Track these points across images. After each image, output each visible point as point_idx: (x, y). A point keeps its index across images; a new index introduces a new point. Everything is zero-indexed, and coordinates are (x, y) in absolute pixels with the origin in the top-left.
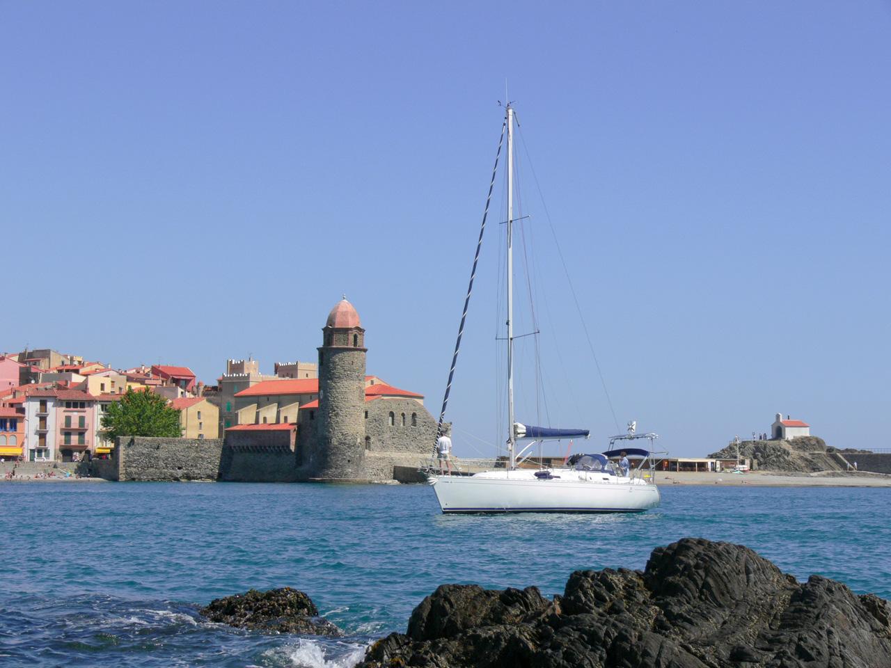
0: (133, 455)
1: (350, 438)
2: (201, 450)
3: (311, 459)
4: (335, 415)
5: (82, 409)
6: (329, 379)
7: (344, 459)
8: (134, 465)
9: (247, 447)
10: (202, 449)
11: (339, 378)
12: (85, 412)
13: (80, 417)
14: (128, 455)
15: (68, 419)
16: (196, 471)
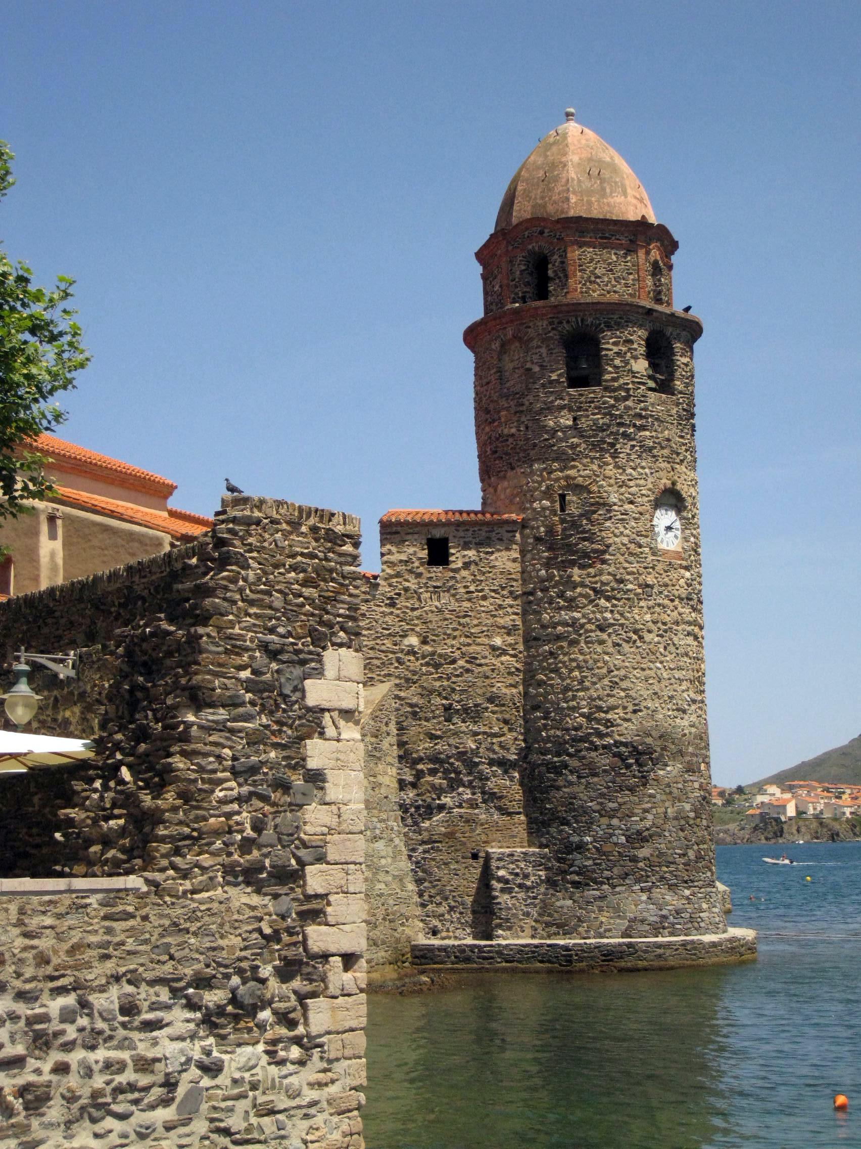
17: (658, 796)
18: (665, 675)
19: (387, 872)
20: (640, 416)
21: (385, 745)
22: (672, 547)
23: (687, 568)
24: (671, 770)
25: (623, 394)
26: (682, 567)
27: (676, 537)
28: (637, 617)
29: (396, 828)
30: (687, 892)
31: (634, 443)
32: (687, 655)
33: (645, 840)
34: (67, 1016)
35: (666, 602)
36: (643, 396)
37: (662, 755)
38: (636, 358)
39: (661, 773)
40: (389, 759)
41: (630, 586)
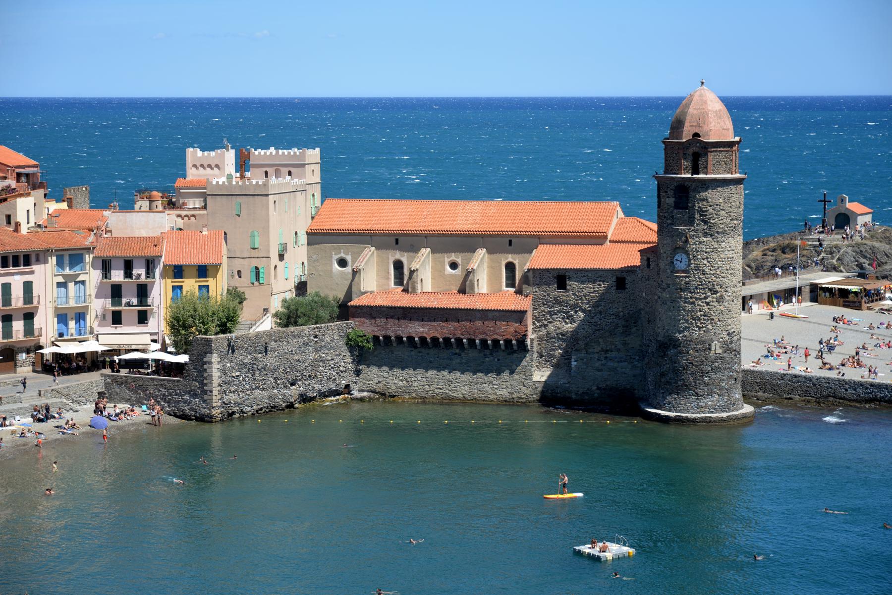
0: (232, 369)
1: (735, 338)
2: (321, 347)
3: (574, 364)
4: (718, 301)
5: (27, 269)
6: (705, 235)
7: (731, 375)
8: (233, 389)
9: (411, 339)
10: (323, 344)
11: (723, 233)
12: (32, 272)
13: (25, 283)
14: (223, 371)
15: (7, 287)
16: (318, 387)
17: (668, 361)
18: (673, 317)
19: (625, 373)
20: (669, 219)
21: (634, 330)
22: (683, 268)
23: (686, 277)
24: (672, 352)
25: (664, 211)
26: (683, 277)
27: (685, 264)
28: (665, 296)
29: (637, 359)
30: (676, 396)
31: (666, 230)
32: (684, 310)
33: (664, 375)
34: (173, 392)
35: (675, 290)
36: (671, 212)
37: (670, 347)
38: (668, 197)
39: (669, 352)
40: (635, 335)
41: (664, 284)
